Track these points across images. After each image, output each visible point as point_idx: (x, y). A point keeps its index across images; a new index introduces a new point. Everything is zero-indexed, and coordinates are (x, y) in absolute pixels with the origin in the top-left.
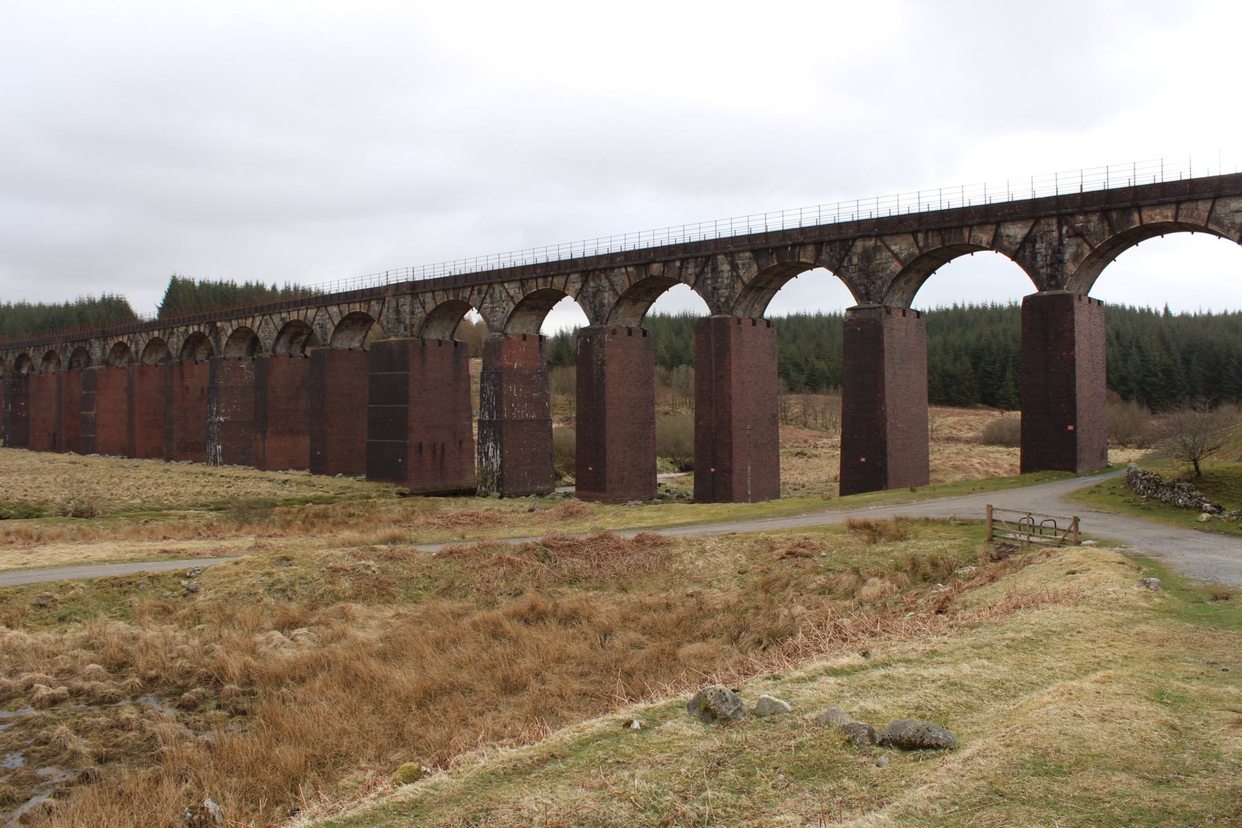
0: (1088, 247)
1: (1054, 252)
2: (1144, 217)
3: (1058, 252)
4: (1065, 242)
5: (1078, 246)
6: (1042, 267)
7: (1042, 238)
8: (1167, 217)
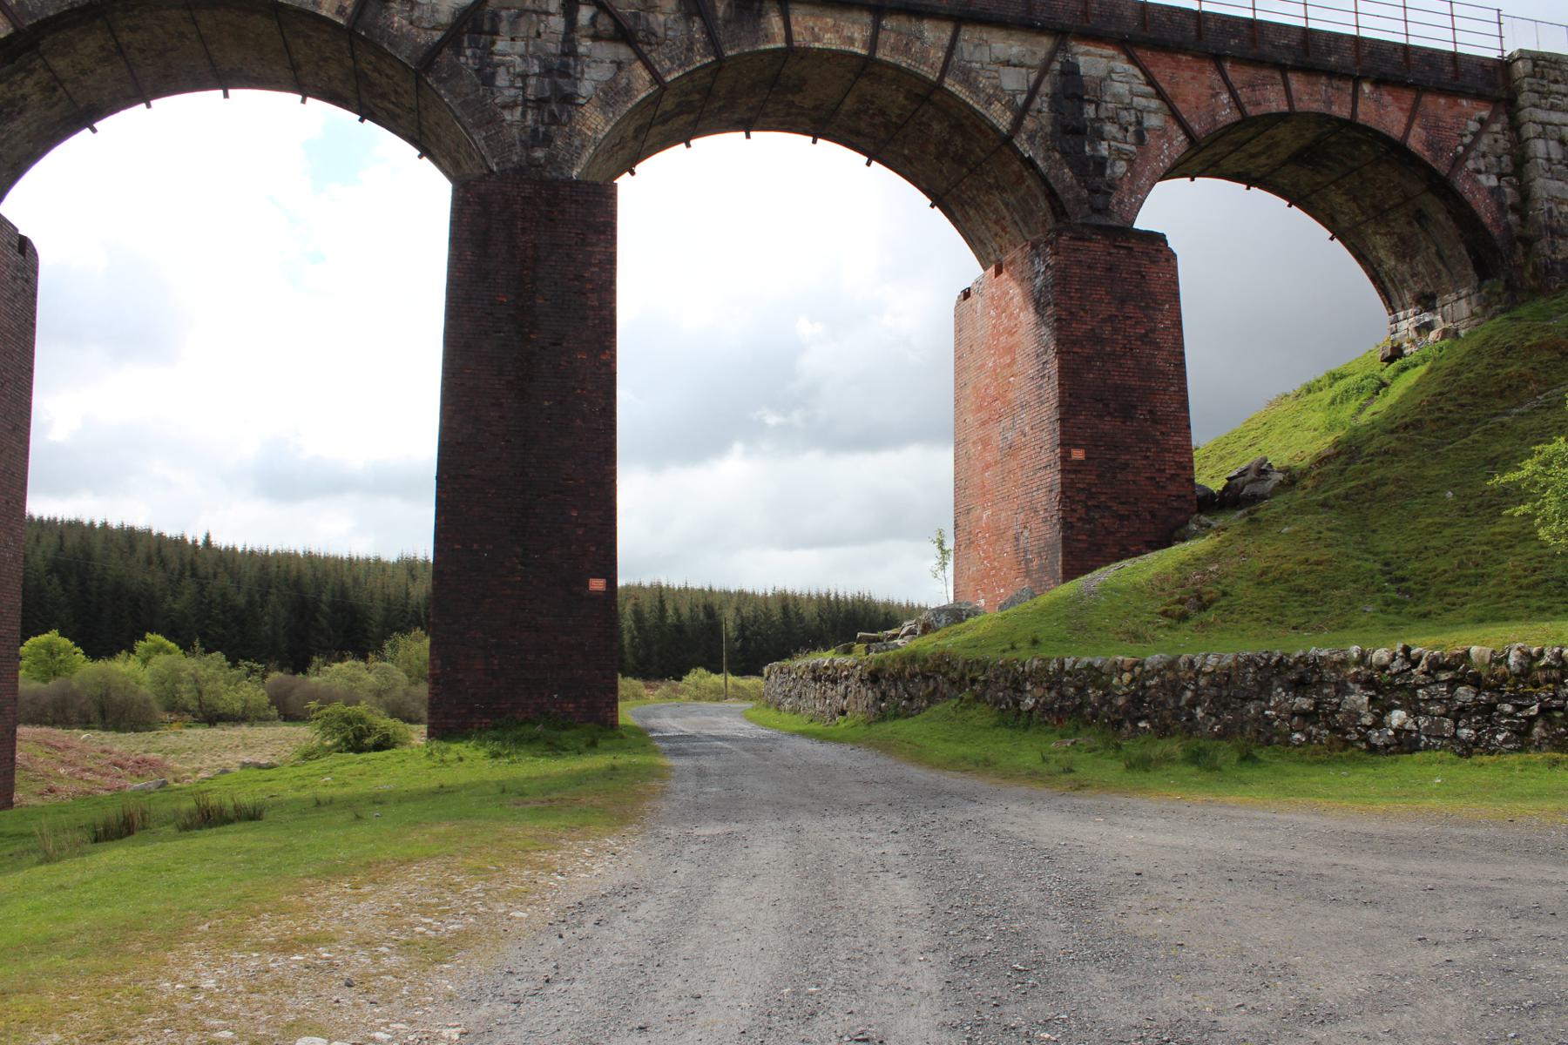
0: (646, 75)
1: (547, 71)
2: (795, 28)
3: (563, 66)
4: (581, 50)
5: (619, 65)
6: (504, 107)
7: (514, 23)
8: (851, 41)
